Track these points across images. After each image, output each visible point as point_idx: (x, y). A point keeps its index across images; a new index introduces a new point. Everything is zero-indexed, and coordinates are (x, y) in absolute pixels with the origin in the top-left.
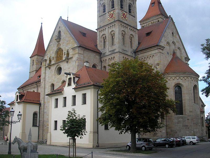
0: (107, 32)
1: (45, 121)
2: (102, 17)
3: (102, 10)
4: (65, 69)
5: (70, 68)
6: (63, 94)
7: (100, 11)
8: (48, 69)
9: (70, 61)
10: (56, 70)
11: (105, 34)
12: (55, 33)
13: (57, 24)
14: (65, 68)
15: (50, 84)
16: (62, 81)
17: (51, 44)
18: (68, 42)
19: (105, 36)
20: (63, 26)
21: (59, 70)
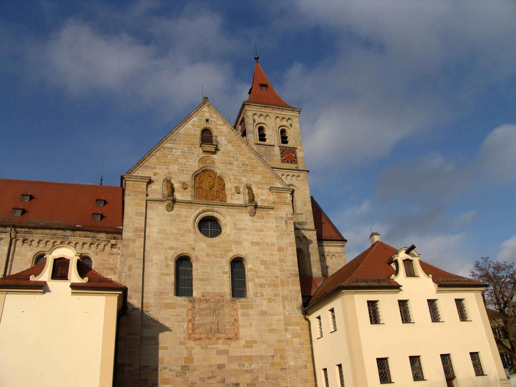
1: (145, 367)
4: (242, 229)
5: (261, 231)
8: (162, 207)
9: (259, 212)
14: (242, 226)
15: (173, 254)
20: (221, 123)
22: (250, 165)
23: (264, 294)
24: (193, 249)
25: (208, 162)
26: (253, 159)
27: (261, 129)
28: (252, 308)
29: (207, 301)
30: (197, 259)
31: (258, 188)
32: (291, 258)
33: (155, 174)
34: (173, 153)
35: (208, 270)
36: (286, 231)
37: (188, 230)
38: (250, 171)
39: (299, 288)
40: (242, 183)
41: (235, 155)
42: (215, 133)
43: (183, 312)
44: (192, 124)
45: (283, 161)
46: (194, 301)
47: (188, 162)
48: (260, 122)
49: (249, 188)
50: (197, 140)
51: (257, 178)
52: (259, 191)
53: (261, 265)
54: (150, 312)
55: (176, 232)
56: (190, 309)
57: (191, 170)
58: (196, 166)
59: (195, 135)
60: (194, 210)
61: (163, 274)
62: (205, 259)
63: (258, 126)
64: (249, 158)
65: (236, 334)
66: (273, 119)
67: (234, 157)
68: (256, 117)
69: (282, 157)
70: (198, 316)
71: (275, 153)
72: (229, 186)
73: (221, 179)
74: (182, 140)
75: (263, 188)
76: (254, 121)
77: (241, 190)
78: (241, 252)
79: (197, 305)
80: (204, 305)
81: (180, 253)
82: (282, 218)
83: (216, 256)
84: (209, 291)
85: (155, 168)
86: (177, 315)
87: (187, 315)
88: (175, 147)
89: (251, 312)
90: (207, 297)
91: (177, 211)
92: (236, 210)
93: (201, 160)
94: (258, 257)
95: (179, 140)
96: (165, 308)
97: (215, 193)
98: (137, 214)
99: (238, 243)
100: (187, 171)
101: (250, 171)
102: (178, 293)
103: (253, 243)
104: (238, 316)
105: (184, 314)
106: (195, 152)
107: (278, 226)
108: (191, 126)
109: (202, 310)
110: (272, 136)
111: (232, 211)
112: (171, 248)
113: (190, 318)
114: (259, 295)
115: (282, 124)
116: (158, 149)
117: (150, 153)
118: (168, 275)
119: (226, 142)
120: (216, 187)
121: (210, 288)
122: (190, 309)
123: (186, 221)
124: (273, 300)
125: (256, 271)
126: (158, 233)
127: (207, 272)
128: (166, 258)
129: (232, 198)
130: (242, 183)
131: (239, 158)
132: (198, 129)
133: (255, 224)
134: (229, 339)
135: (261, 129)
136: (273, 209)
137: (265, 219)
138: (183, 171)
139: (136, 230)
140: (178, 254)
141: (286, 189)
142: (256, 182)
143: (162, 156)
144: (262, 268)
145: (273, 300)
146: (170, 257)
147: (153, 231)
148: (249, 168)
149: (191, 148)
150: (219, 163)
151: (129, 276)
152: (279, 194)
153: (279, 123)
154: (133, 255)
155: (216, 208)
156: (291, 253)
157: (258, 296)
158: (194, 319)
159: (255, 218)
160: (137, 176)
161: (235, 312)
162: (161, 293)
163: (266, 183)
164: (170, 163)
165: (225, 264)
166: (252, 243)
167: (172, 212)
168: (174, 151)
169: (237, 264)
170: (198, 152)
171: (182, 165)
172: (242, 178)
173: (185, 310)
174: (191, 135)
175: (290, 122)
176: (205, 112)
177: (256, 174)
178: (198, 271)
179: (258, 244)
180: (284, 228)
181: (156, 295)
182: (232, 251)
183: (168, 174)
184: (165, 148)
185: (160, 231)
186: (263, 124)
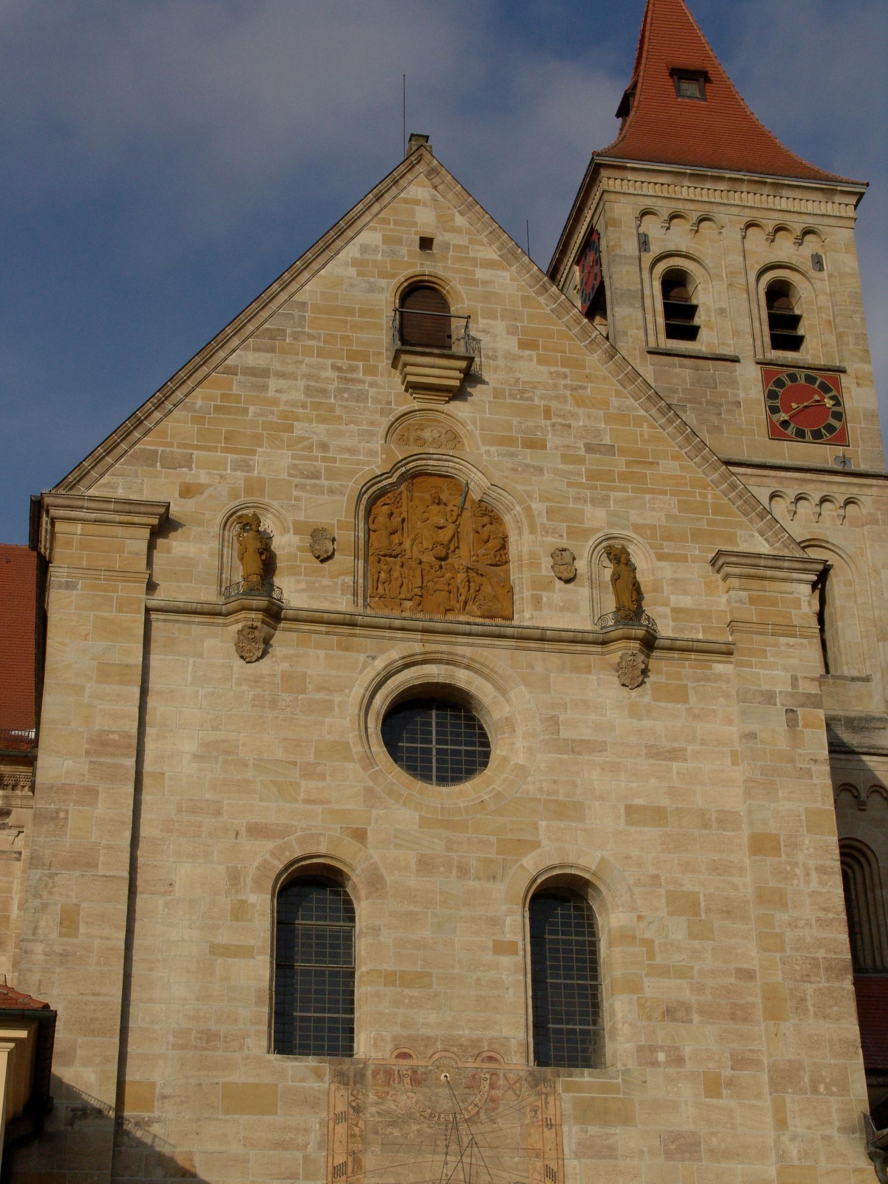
5: (675, 755)
8: (217, 643)
14: (586, 733)
20: (492, 254)
22: (623, 452)
23: (687, 1051)
24: (360, 835)
25: (427, 434)
27: (674, 282)
28: (627, 1120)
29: (417, 1079)
30: (376, 882)
31: (661, 557)
32: (814, 885)
33: (187, 491)
34: (271, 393)
36: (792, 761)
37: (339, 749)
38: (624, 477)
39: (851, 1029)
40: (586, 533)
41: (554, 404)
42: (461, 299)
43: (307, 1130)
44: (355, 263)
45: (778, 431)
46: (360, 1077)
47: (340, 434)
48: (672, 247)
50: (382, 335)
51: (657, 511)
52: (666, 570)
53: (672, 913)
54: (156, 1129)
55: (279, 754)
56: (339, 1118)
58: (373, 454)
59: (371, 312)
60: (362, 658)
61: (217, 950)
63: (661, 267)
66: (733, 233)
68: (652, 227)
69: (774, 410)
70: (376, 1148)
71: (742, 396)
72: (528, 547)
73: (488, 514)
74: (311, 337)
75: (684, 559)
76: (644, 243)
77: (581, 565)
78: (580, 855)
79: (372, 1098)
80: (405, 1099)
81: (298, 853)
82: (769, 697)
83: (463, 871)
84: (431, 1033)
85: (187, 462)
86: (279, 1145)
87: (326, 1142)
88: (277, 365)
89: (627, 1138)
90: (418, 1062)
91: (286, 658)
92: (555, 658)
93: (399, 428)
94: (656, 877)
95: (296, 336)
96: (227, 1111)
97: (461, 577)
98: (106, 672)
99: (566, 810)
101: (624, 477)
102: (285, 1041)
104: (560, 1157)
105: (314, 1137)
106: (372, 392)
107: (753, 736)
108: (352, 271)
109: (393, 1124)
110: (729, 316)
111: (541, 661)
112: (257, 831)
113: (339, 1160)
114: (661, 1056)
116: (199, 375)
117: (163, 396)
118: (244, 952)
119: (512, 344)
120: (464, 550)
121: (433, 1018)
122: (339, 1118)
123: (327, 707)
124: (730, 1083)
125: (649, 944)
126: (197, 757)
128: (235, 877)
129: (537, 602)
130: (586, 533)
131: (575, 416)
132: (383, 283)
135: (674, 282)
137: (693, 699)
138: (316, 476)
139: (100, 744)
140: (288, 857)
141: (793, 559)
142: (653, 528)
144: (678, 929)
145: (730, 1083)
146: (252, 871)
147: (175, 752)
148: (620, 463)
149: (353, 369)
150: (479, 441)
151: (64, 957)
152: (755, 584)
153: (762, 250)
154: (84, 860)
155: (464, 649)
156: (812, 864)
157: (654, 1063)
158: (358, 1164)
159: (644, 696)
160: (107, 501)
161: (549, 1134)
162: (209, 1037)
163: (697, 535)
164: (257, 439)
165: (504, 908)
166: (630, 810)
167: (264, 666)
168: (273, 384)
169: (561, 907)
170: (386, 388)
171: (310, 448)
172: (588, 509)
173: (315, 1122)
174: (350, 311)
175: (811, 245)
176: (417, 202)
177: (652, 491)
179: (657, 815)
180: (783, 744)
181: (183, 1047)
182: (536, 845)
183: (249, 491)
184: (232, 371)
185: (209, 751)
186: (687, 257)
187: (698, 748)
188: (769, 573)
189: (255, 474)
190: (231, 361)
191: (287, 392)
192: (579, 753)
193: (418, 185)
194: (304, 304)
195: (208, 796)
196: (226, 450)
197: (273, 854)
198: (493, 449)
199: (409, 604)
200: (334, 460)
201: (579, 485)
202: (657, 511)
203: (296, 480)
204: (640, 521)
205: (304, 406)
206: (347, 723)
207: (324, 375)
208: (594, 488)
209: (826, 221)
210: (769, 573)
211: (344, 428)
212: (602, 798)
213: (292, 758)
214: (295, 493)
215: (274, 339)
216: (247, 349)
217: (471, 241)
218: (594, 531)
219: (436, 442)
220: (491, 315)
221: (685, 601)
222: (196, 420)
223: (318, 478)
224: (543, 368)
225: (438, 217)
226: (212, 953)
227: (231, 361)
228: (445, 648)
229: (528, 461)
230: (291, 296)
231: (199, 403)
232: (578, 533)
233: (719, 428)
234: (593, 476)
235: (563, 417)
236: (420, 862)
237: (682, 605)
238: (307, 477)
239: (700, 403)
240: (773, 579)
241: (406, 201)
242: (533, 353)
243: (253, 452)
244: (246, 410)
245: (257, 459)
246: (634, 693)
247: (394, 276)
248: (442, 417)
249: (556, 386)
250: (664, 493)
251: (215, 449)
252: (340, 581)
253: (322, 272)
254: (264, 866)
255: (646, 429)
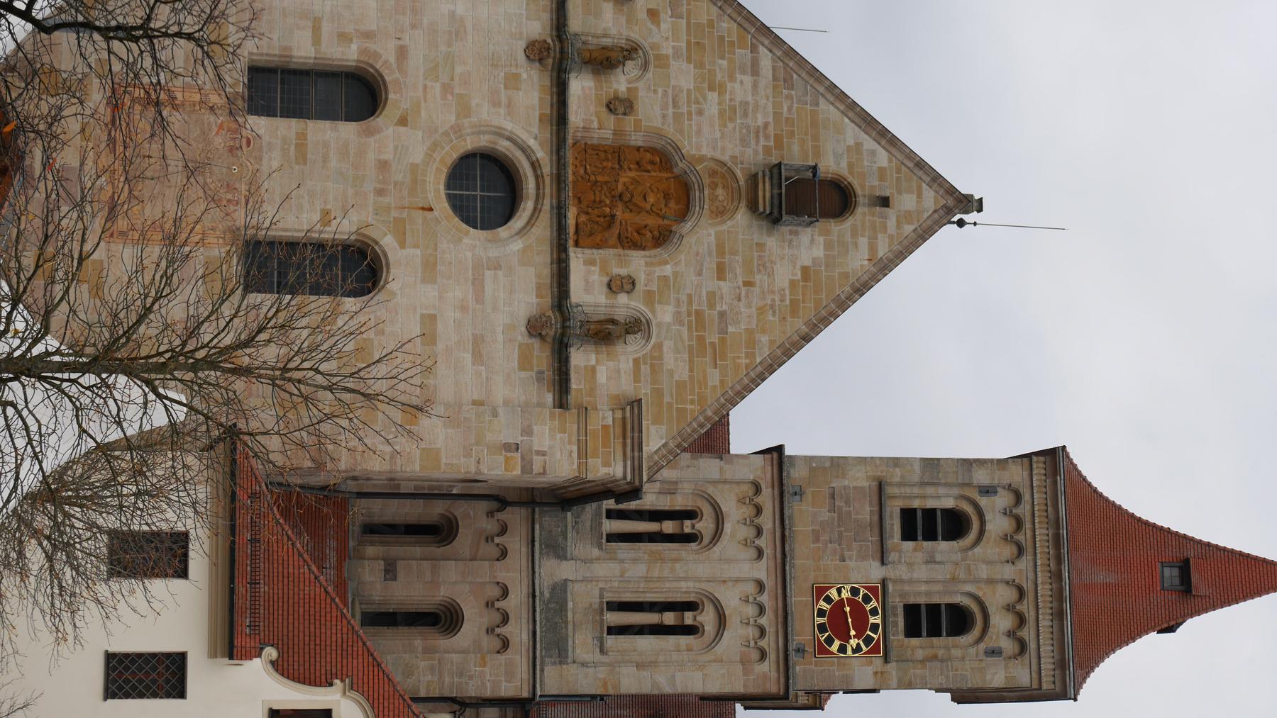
0: (726, 571)
2: (865, 512)
3: (930, 504)
5: (478, 356)
6: (213, 654)
7: (930, 490)
9: (542, 356)
10: (503, 146)
11: (717, 549)
12: (852, 133)
13: (921, 164)
15: (385, 59)
16: (388, 242)
17: (766, 60)
18: (712, 337)
19: (706, 540)
21: (484, 188)
22: (723, 341)
24: (403, 121)
25: (720, 192)
26: (750, 355)
30: (370, 133)
31: (636, 361)
35: (333, 163)
36: (477, 443)
37: (464, 109)
38: (701, 339)
41: (757, 290)
44: (858, 145)
48: (988, 517)
49: (636, 326)
51: (675, 364)
55: (459, 70)
57: (681, 132)
60: (535, 130)
62: (371, 156)
63: (969, 509)
64: (752, 343)
65: (123, 234)
66: (1008, 572)
67: (748, 284)
71: (851, 564)
72: (637, 263)
73: (662, 238)
74: (790, 109)
75: (637, 378)
76: (988, 491)
77: (623, 299)
80: (219, 141)
82: (528, 431)
83: (380, 192)
85: (676, 15)
92: (546, 272)
93: (722, 172)
95: (789, 97)
100: (677, 117)
101: (701, 339)
103: (430, 321)
107: (495, 415)
108: (851, 142)
112: (402, 52)
115: (991, 610)
116: (747, 25)
118: (317, 40)
120: (628, 215)
123: (496, 104)
126: (452, 14)
127: (325, 159)
128: (368, 35)
129: (590, 262)
131: (749, 305)
132: (844, 164)
133: (500, 338)
134: (112, 209)
136: (562, 403)
137: (523, 375)
138: (675, 105)
140: (385, 73)
141: (640, 458)
142: (661, 358)
143: (721, 38)
148: (712, 337)
149: (767, 137)
152: (619, 430)
153: (998, 597)
159: (521, 334)
164: (700, 65)
166: (433, 318)
168: (748, 79)
170: (747, 154)
171: (697, 102)
174: (816, 138)
175: (1008, 646)
176: (920, 196)
177: (691, 361)
178: (332, 136)
180: (490, 437)
182: (402, 245)
183: (658, 57)
184: (754, 49)
187: (484, 375)
188: (629, 441)
189: (672, 62)
190: (761, 48)
191: (741, 88)
192: (473, 284)
193: (935, 198)
194: (817, 105)
195: (425, 21)
196: (689, 43)
197: (386, 62)
198: (713, 238)
199: (582, 171)
200: (690, 119)
201: (690, 302)
202: (675, 364)
203: (670, 91)
204: (665, 349)
205: (731, 100)
206: (485, 116)
207: (760, 116)
208: (689, 314)
209: (1034, 661)
210: (629, 441)
211: (717, 128)
212: (440, 297)
213: (456, 78)
214: (660, 91)
215: (785, 81)
216: (773, 61)
217: (891, 237)
218: (653, 312)
219: (713, 198)
220: (828, 246)
221: (602, 377)
222: (711, 24)
223: (674, 107)
224: (786, 284)
225: (909, 212)
226: (315, 19)
227: (761, 48)
228: (548, 190)
229: (705, 265)
230: (823, 95)
231: (725, 25)
232: (649, 298)
233: (817, 540)
234: (699, 314)
235: (747, 296)
236: (386, 162)
237: (598, 375)
238: (674, 100)
239: (839, 526)
240: (624, 445)
241: (919, 188)
242: (799, 277)
243: (689, 60)
244: (722, 58)
245: (684, 65)
246: (523, 329)
247: (851, 174)
248: (735, 203)
249: (773, 292)
250: (691, 370)
251: (688, 34)
252: (594, 118)
253: (847, 120)
254: (376, 55)
255: (744, 361)
